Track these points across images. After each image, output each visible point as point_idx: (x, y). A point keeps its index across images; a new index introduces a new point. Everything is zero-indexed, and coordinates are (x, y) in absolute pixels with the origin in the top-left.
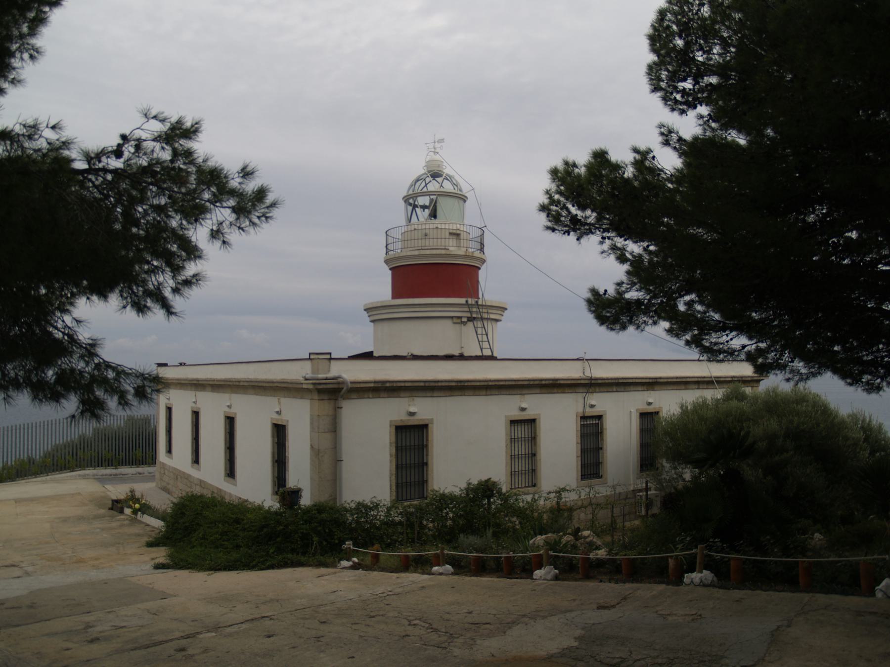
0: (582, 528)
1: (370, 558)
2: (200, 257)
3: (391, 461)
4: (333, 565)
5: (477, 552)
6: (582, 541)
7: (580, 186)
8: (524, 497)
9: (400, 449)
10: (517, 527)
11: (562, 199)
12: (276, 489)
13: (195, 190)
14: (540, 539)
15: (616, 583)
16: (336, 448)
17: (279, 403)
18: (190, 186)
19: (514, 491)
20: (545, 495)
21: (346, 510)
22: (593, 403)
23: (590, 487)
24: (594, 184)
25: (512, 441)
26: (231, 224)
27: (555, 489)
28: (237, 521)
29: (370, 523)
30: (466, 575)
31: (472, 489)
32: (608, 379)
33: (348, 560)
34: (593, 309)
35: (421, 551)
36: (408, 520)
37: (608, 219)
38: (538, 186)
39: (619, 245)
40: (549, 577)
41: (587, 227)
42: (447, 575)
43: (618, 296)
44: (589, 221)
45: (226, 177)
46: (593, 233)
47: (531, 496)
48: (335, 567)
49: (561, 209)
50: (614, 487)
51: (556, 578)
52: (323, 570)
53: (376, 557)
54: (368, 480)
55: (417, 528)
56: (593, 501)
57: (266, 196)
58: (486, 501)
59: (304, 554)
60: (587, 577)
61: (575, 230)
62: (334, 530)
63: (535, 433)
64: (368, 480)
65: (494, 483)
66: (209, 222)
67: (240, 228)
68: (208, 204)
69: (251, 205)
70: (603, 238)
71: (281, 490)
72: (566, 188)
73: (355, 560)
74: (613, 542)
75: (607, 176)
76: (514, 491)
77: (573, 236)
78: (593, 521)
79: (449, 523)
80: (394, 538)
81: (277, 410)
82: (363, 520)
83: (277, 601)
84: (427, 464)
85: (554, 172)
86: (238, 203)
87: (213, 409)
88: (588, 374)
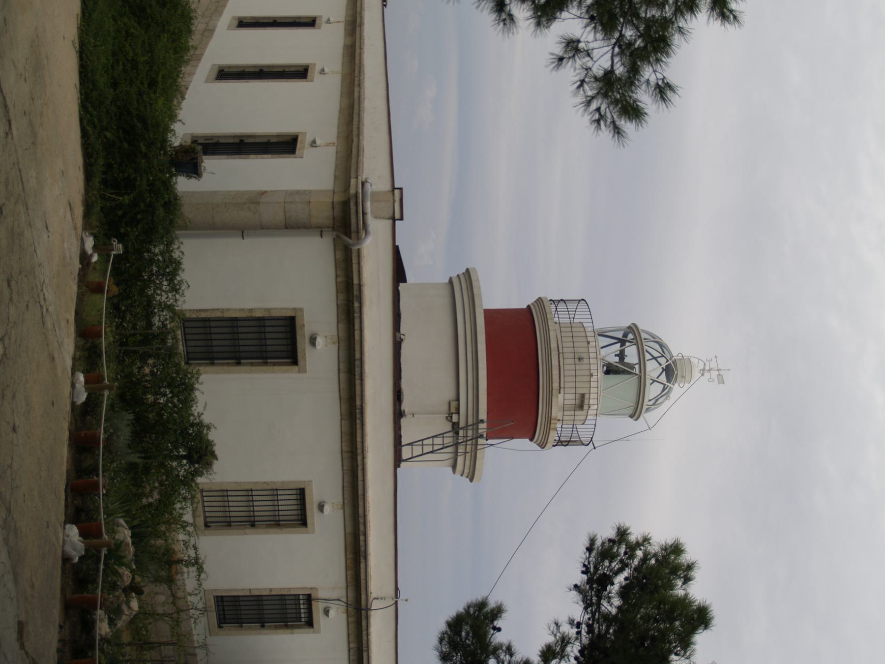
0: (143, 597)
1: (97, 280)
2: (538, 24)
3: (242, 310)
4: (87, 226)
5: (107, 440)
6: (123, 598)
7: (657, 588)
8: (189, 510)
9: (260, 324)
10: (144, 501)
11: (636, 562)
12: (200, 141)
13: (638, 16)
14: (125, 534)
15: (59, 651)
16: (262, 228)
17: (328, 145)
18: (643, 9)
19: (199, 496)
20: (192, 542)
21: (170, 244)
22: (332, 613)
23: (205, 610)
24: (659, 608)
25: (274, 492)
26: (588, 69)
27: (202, 557)
28: (153, 84)
29: (150, 280)
30: (71, 423)
31: (200, 432)
32: (368, 635)
33: (95, 248)
34: (472, 611)
35: (108, 356)
36: (155, 336)
37: (607, 631)
38: (655, 528)
39: (569, 649)
40: (68, 549)
41: (594, 599)
42: (72, 394)
43: (491, 648)
44: (604, 603)
45: (658, 60)
46: (586, 608)
47: (191, 520)
48: (85, 228)
49: (621, 561)
50: (204, 646)
51: (66, 559)
52: (79, 210)
53: (98, 289)
54: (214, 278)
55: (142, 349)
56: (183, 615)
57: (630, 119)
58: (182, 452)
59: (104, 182)
60: (67, 607)
61: (590, 581)
62: (139, 227)
63: (286, 526)
64: (214, 278)
65: (209, 465)
66: (591, 37)
67: (582, 82)
68: (617, 35)
69: (617, 98)
70: (579, 625)
71: (199, 148)
72: (652, 567)
73: (95, 258)
74: (120, 645)
75: (672, 629)
76: (199, 496)
77: (580, 578)
78: (153, 614)
79: (150, 398)
80: (128, 317)
81: (318, 142)
82: (155, 269)
83: (34, 143)
84: (239, 364)
85: (676, 549)
86: (620, 79)
87: (321, 48)
88: (375, 605)
